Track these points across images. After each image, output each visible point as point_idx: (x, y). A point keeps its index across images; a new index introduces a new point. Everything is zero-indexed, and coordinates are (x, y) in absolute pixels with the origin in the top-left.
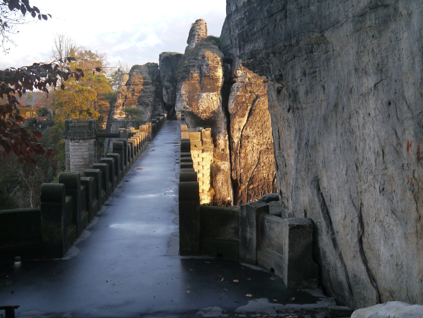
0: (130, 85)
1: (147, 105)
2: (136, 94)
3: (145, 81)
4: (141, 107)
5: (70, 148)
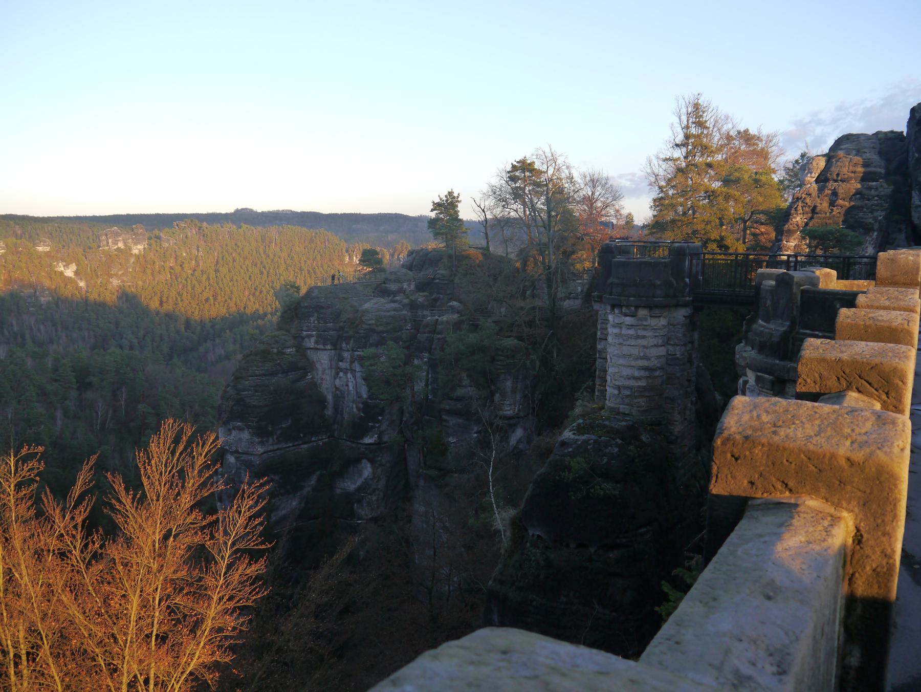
0: (826, 180)
1: (868, 229)
2: (840, 202)
3: (868, 169)
5: (610, 330)
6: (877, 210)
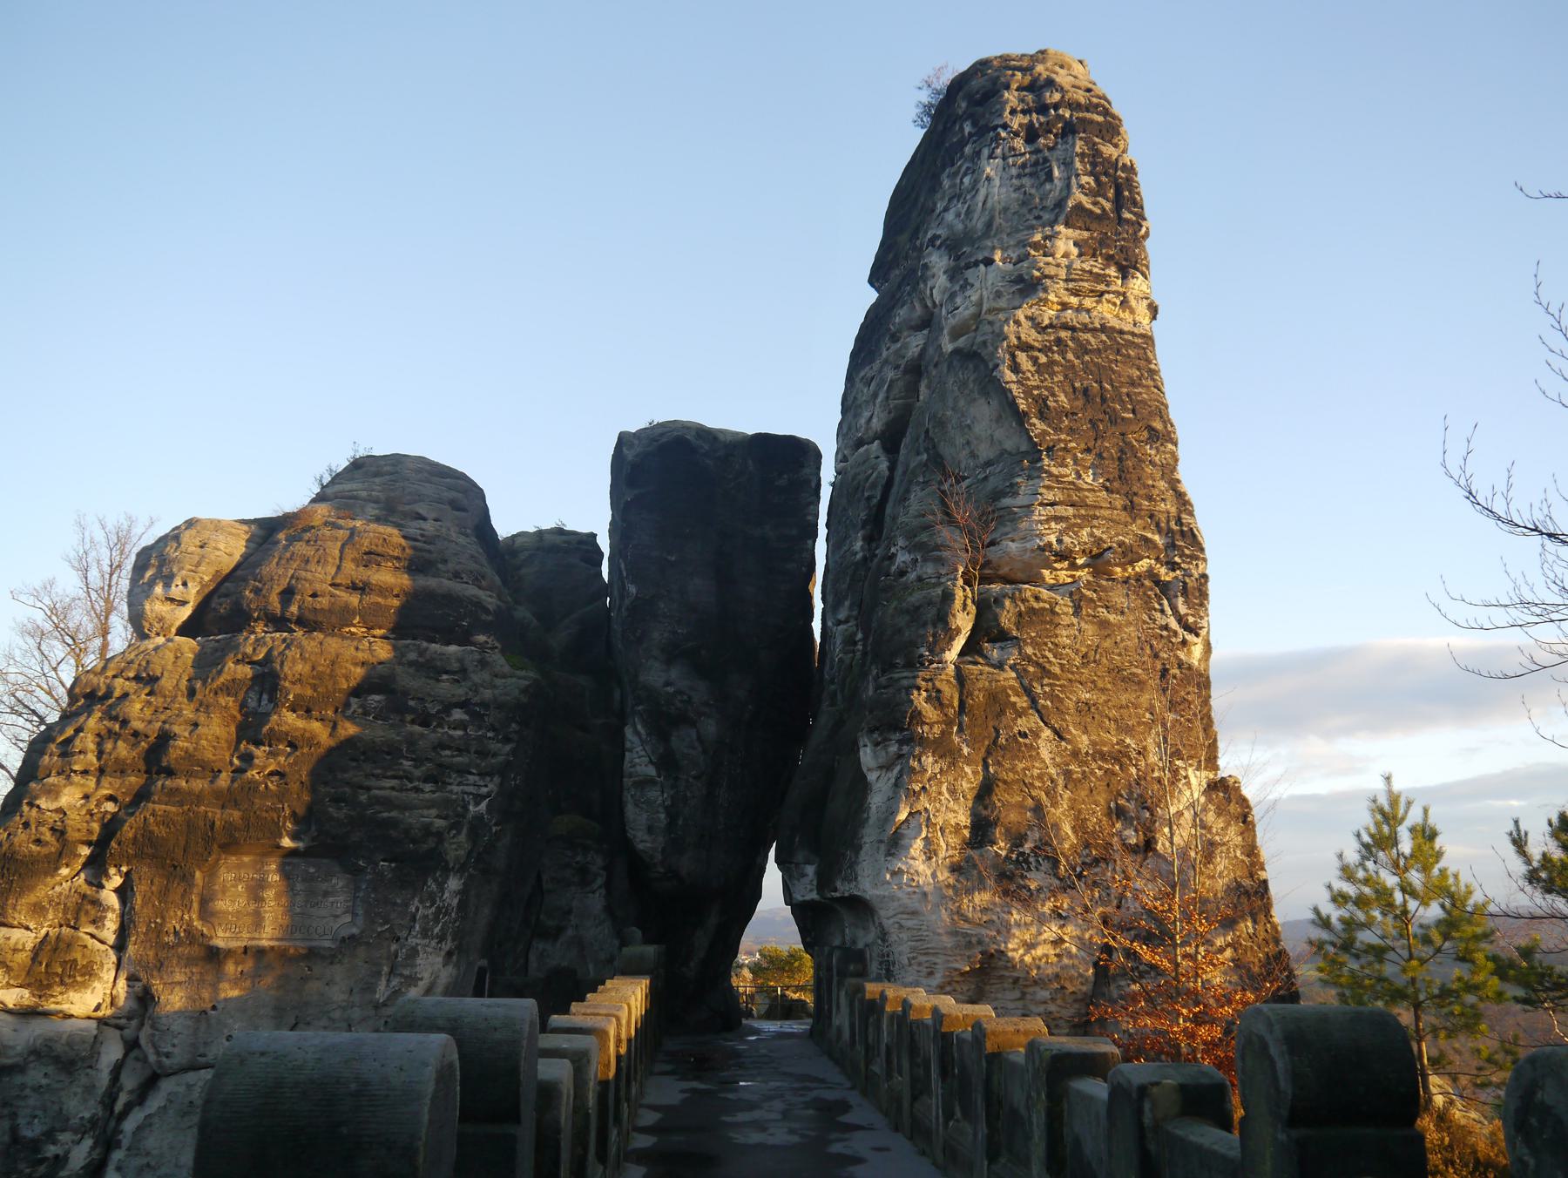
0: (238, 620)
1: (416, 862)
2: (290, 720)
3: (431, 582)
4: (339, 882)
6: (463, 771)
